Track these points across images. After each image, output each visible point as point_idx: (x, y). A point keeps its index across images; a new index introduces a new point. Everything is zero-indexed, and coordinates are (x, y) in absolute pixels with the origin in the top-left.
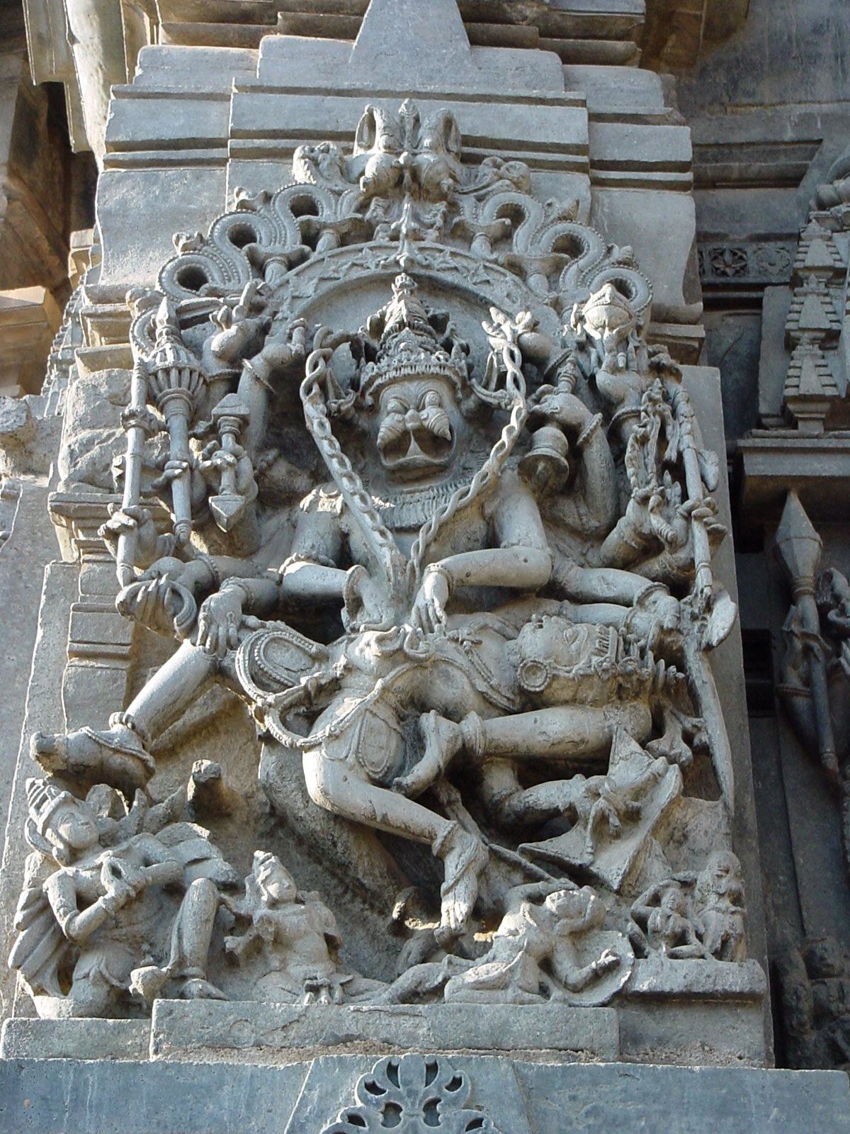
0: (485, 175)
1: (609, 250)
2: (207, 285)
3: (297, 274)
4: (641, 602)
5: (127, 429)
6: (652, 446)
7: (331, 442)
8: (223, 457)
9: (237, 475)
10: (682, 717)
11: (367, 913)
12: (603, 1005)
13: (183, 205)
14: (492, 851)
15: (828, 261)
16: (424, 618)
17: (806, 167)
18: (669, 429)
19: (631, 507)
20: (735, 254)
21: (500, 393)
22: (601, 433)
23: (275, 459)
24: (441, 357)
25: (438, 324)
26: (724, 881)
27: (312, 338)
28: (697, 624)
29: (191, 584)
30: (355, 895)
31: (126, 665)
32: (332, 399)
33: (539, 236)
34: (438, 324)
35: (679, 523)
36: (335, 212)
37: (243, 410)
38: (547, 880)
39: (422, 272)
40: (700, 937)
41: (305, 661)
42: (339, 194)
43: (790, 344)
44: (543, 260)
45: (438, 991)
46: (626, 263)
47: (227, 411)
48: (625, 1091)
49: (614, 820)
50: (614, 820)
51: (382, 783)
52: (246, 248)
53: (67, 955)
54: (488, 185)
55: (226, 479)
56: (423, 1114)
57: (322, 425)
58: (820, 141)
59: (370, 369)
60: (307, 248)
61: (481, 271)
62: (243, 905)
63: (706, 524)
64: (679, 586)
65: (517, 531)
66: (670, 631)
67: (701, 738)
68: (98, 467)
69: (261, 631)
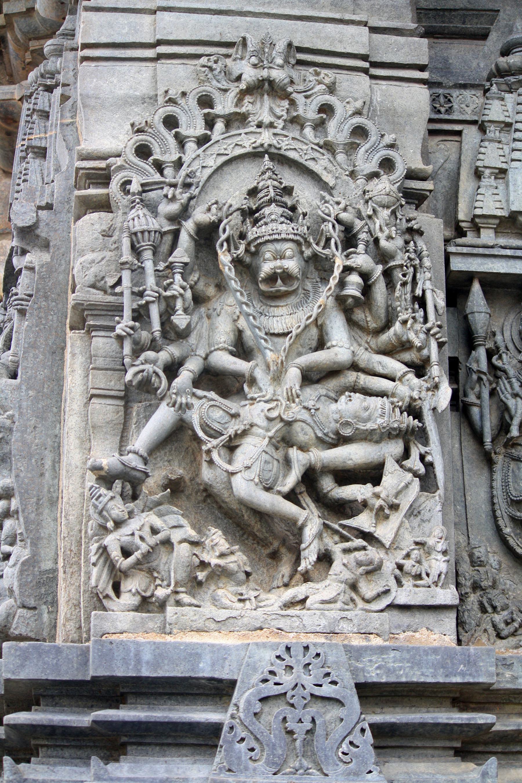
0: (310, 81)
1: (382, 136)
2: (152, 158)
3: (204, 151)
4: (400, 379)
5: (122, 269)
6: (409, 287)
7: (235, 281)
8: (176, 289)
9: (184, 300)
10: (420, 446)
11: (256, 545)
12: (382, 611)
13: (131, 92)
14: (324, 523)
15: (502, 118)
16: (290, 394)
17: (489, 28)
18: (418, 276)
19: (397, 327)
20: (446, 97)
21: (326, 251)
22: (382, 278)
23: (198, 279)
24: (295, 228)
25: (288, 191)
26: (440, 544)
27: (220, 209)
28: (430, 393)
29: (162, 367)
30: (249, 535)
31: (122, 403)
32: (233, 251)
33: (342, 126)
34: (288, 191)
35: (422, 336)
36: (225, 105)
37: (186, 260)
38: (352, 540)
39: (276, 151)
40: (428, 575)
41: (227, 418)
42: (226, 91)
43: (478, 175)
44: (345, 144)
45: (303, 601)
46: (392, 146)
47: (177, 260)
48: (394, 657)
49: (387, 511)
50: (387, 511)
51: (268, 489)
52: (173, 131)
53: (115, 575)
54: (312, 89)
55: (179, 304)
56: (302, 671)
57: (230, 269)
58: (498, 11)
59: (252, 233)
60: (209, 133)
61: (310, 151)
62: (206, 557)
63: (437, 339)
64: (420, 369)
65: (336, 338)
66: (415, 400)
67: (429, 458)
68: (99, 278)
69: (204, 400)
